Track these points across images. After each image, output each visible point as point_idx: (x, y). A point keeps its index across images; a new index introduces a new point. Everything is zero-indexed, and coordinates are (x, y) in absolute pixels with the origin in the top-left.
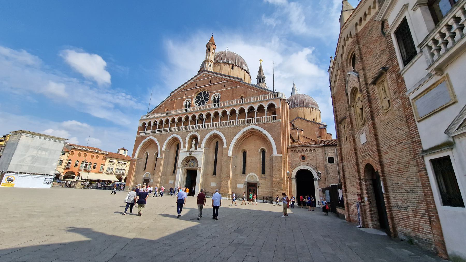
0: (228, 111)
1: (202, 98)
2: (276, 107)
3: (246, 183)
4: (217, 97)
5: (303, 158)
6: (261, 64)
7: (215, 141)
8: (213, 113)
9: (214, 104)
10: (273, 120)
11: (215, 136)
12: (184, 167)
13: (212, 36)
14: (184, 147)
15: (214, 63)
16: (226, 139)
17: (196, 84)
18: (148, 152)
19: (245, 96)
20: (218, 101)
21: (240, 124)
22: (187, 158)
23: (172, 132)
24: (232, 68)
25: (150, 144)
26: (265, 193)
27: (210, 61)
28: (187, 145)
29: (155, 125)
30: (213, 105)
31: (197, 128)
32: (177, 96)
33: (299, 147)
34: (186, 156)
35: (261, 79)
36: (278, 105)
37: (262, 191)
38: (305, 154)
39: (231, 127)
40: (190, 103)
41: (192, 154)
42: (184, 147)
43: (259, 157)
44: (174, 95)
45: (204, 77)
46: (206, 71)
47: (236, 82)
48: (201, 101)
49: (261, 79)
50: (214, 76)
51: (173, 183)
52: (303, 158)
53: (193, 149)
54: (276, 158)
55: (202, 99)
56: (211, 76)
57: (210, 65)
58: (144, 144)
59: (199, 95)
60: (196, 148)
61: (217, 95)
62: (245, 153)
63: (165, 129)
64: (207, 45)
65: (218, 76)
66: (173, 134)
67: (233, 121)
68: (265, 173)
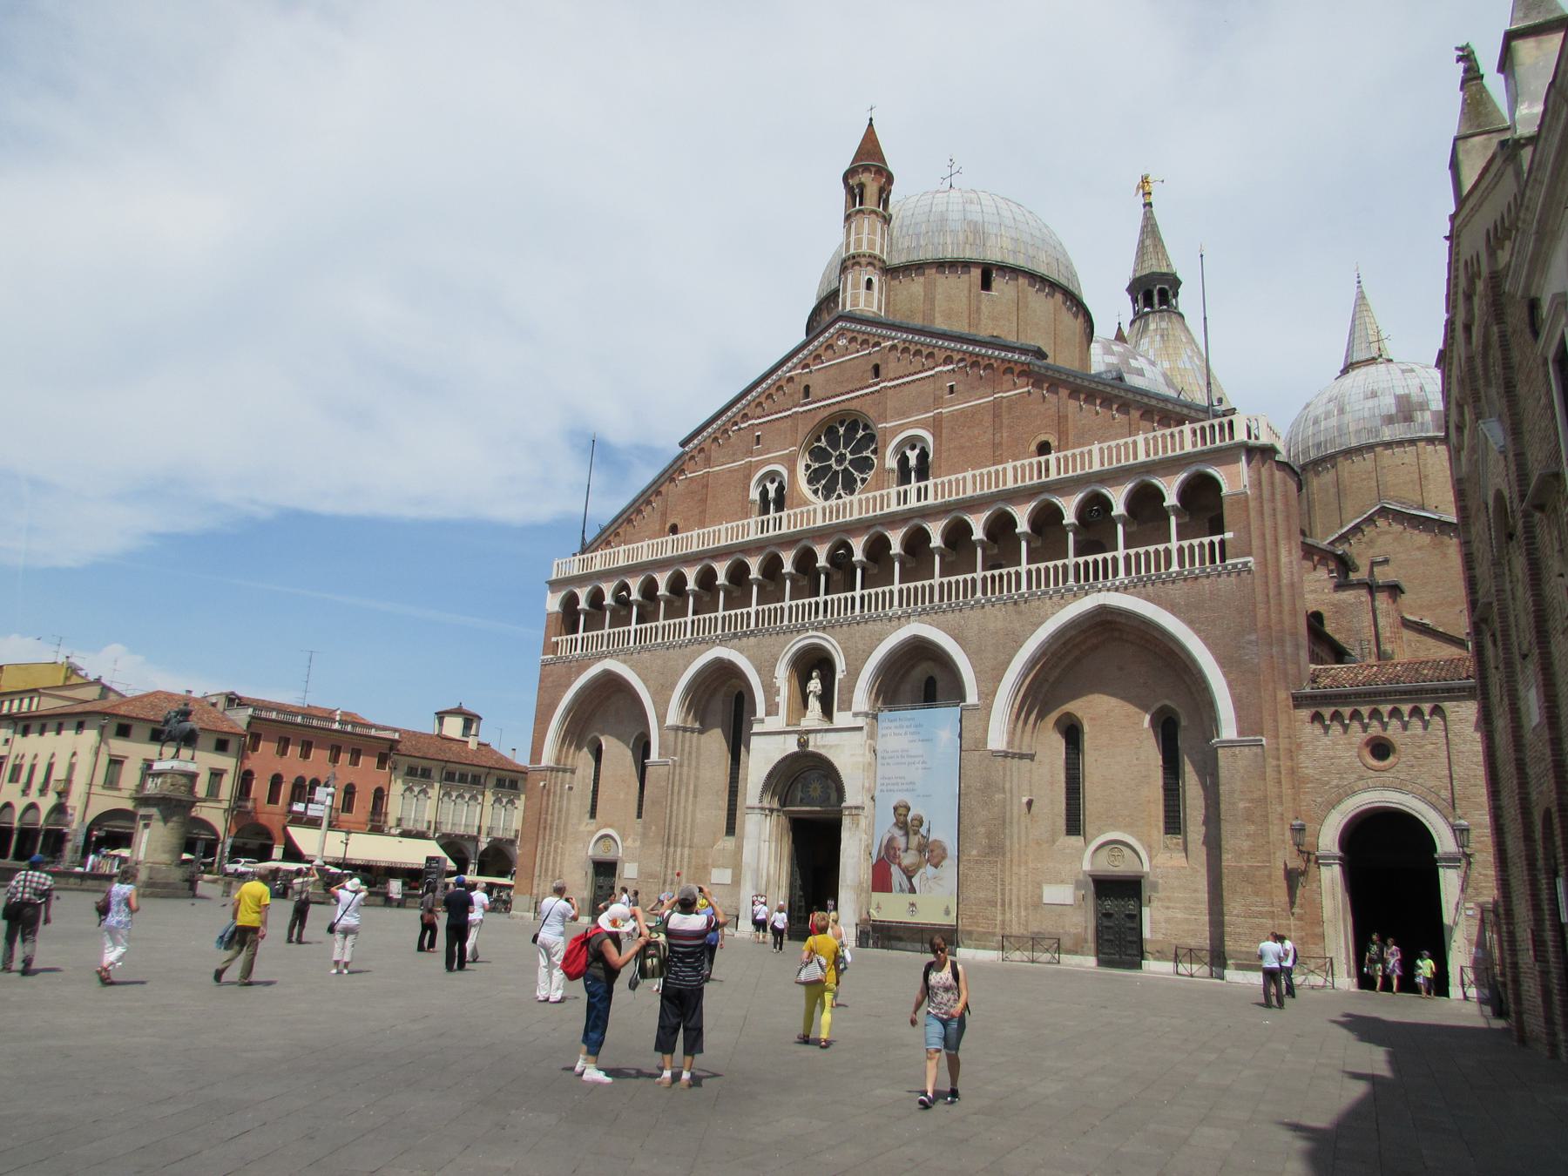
0: (978, 521)
2: (1225, 490)
3: (1087, 882)
5: (1381, 749)
6: (1148, 205)
9: (902, 489)
10: (1213, 561)
11: (919, 652)
12: (776, 805)
13: (871, 125)
14: (772, 710)
16: (974, 667)
17: (807, 388)
20: (923, 473)
21: (1043, 587)
24: (986, 284)
26: (1186, 927)
27: (870, 260)
28: (782, 699)
29: (623, 602)
30: (899, 494)
31: (825, 611)
34: (784, 755)
35: (1155, 292)
36: (1234, 479)
37: (1167, 921)
38: (1393, 731)
41: (811, 743)
42: (772, 710)
45: (846, 350)
46: (851, 318)
48: (837, 472)
49: (1155, 292)
51: (729, 882)
52: (1381, 749)
54: (1234, 755)
56: (877, 344)
57: (869, 282)
59: (823, 443)
60: (827, 712)
62: (1072, 733)
63: (672, 622)
64: (846, 178)
66: (712, 643)
67: (1004, 571)
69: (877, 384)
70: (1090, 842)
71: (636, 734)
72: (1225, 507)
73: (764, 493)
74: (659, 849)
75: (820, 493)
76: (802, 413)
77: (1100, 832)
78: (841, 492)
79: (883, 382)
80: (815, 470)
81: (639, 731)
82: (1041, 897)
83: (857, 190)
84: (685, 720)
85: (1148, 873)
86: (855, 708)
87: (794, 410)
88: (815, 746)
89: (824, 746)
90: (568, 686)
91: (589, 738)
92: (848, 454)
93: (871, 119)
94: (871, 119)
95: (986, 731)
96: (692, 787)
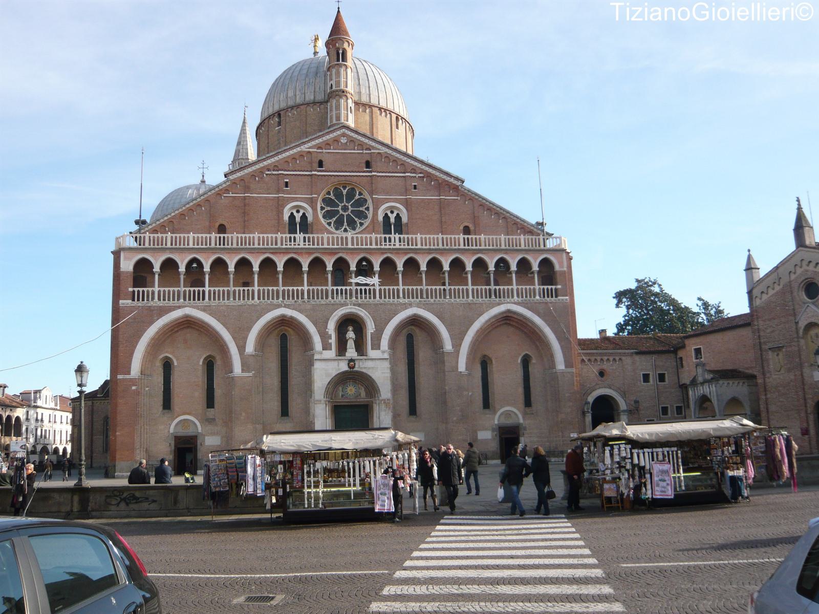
0: (446, 261)
1: (345, 209)
7: (405, 332)
8: (403, 260)
11: (415, 322)
13: (339, 12)
15: (357, 104)
16: (449, 332)
18: (170, 356)
19: (475, 228)
24: (397, 128)
25: (177, 331)
32: (252, 186)
33: (597, 353)
38: (605, 366)
39: (457, 304)
40: (304, 217)
41: (356, 366)
44: (242, 179)
45: (345, 146)
47: (449, 184)
50: (379, 149)
52: (602, 374)
53: (351, 352)
54: (564, 376)
55: (345, 209)
58: (160, 330)
59: (332, 196)
62: (485, 364)
65: (394, 153)
66: (279, 306)
68: (533, 405)
69: (371, 172)
71: (205, 356)
73: (292, 217)
74: (250, 426)
75: (332, 225)
78: (347, 227)
79: (375, 172)
80: (328, 211)
82: (477, 436)
83: (341, 52)
85: (522, 424)
86: (382, 348)
87: (313, 173)
89: (365, 368)
92: (350, 207)
93: (339, 8)
94: (339, 8)
95: (457, 362)
96: (261, 389)
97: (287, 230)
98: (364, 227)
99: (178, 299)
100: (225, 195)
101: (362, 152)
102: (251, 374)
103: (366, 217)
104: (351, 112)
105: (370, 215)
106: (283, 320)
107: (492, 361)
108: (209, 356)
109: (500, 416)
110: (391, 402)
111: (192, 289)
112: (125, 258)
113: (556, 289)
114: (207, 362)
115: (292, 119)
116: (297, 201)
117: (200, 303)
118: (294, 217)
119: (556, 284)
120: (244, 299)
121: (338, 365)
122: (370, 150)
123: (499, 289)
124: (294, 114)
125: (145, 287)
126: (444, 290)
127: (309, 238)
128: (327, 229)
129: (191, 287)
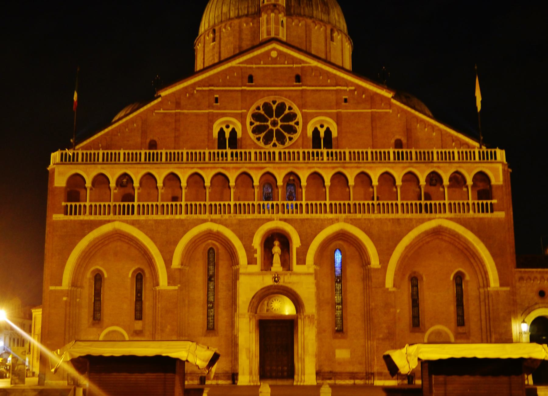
1: (274, 124)
2: (493, 182)
4: (325, 128)
12: (254, 314)
16: (376, 246)
19: (408, 140)
22: (263, 290)
23: (203, 216)
24: (332, 39)
28: (258, 255)
32: (183, 102)
40: (233, 132)
41: (281, 280)
43: (452, 291)
53: (277, 266)
57: (282, 21)
58: (91, 243)
60: (286, 264)
61: (322, 121)
66: (204, 221)
70: (427, 330)
71: (133, 269)
72: (494, 190)
73: (221, 132)
76: (249, 91)
77: (432, 325)
80: (257, 126)
81: (137, 267)
84: (182, 264)
87: (244, 88)
88: (284, 282)
89: (290, 283)
90: (84, 235)
91: (93, 268)
92: (279, 121)
97: (216, 145)
98: (293, 141)
99: (109, 214)
100: (156, 111)
101: (292, 66)
102: (176, 288)
103: (295, 131)
104: (282, 26)
105: (299, 129)
106: (210, 233)
107: (422, 278)
108: (139, 269)
109: (430, 335)
110: (316, 317)
111: (122, 204)
112: (60, 174)
113: (491, 203)
114: (135, 275)
115: (225, 35)
116: (226, 116)
117: (130, 217)
118: (224, 133)
119: (492, 199)
120: (172, 213)
121: (263, 280)
122: (301, 64)
123: (431, 204)
124: (228, 30)
125: (78, 201)
126: (373, 204)
127: (237, 153)
128: (255, 143)
129: (122, 201)
